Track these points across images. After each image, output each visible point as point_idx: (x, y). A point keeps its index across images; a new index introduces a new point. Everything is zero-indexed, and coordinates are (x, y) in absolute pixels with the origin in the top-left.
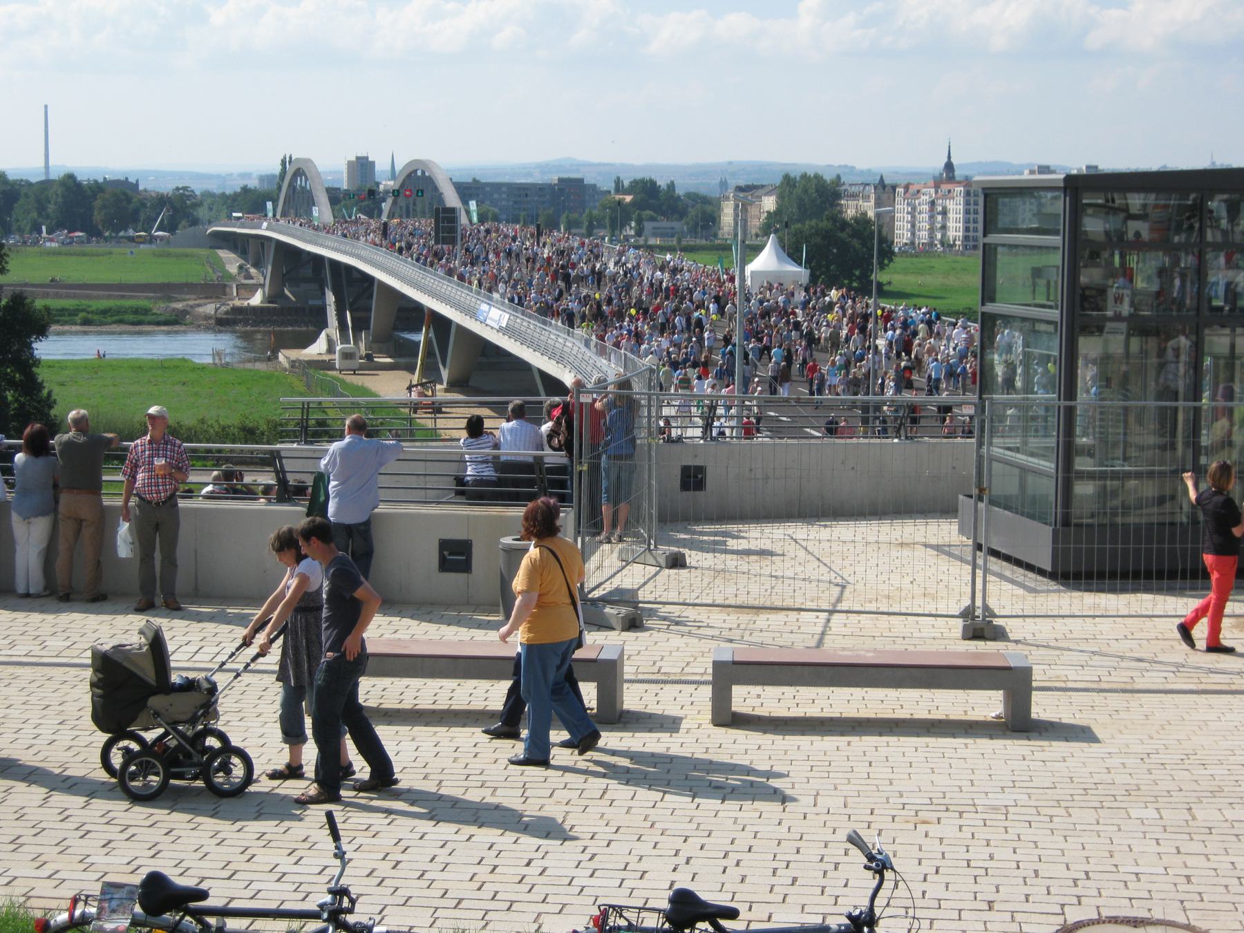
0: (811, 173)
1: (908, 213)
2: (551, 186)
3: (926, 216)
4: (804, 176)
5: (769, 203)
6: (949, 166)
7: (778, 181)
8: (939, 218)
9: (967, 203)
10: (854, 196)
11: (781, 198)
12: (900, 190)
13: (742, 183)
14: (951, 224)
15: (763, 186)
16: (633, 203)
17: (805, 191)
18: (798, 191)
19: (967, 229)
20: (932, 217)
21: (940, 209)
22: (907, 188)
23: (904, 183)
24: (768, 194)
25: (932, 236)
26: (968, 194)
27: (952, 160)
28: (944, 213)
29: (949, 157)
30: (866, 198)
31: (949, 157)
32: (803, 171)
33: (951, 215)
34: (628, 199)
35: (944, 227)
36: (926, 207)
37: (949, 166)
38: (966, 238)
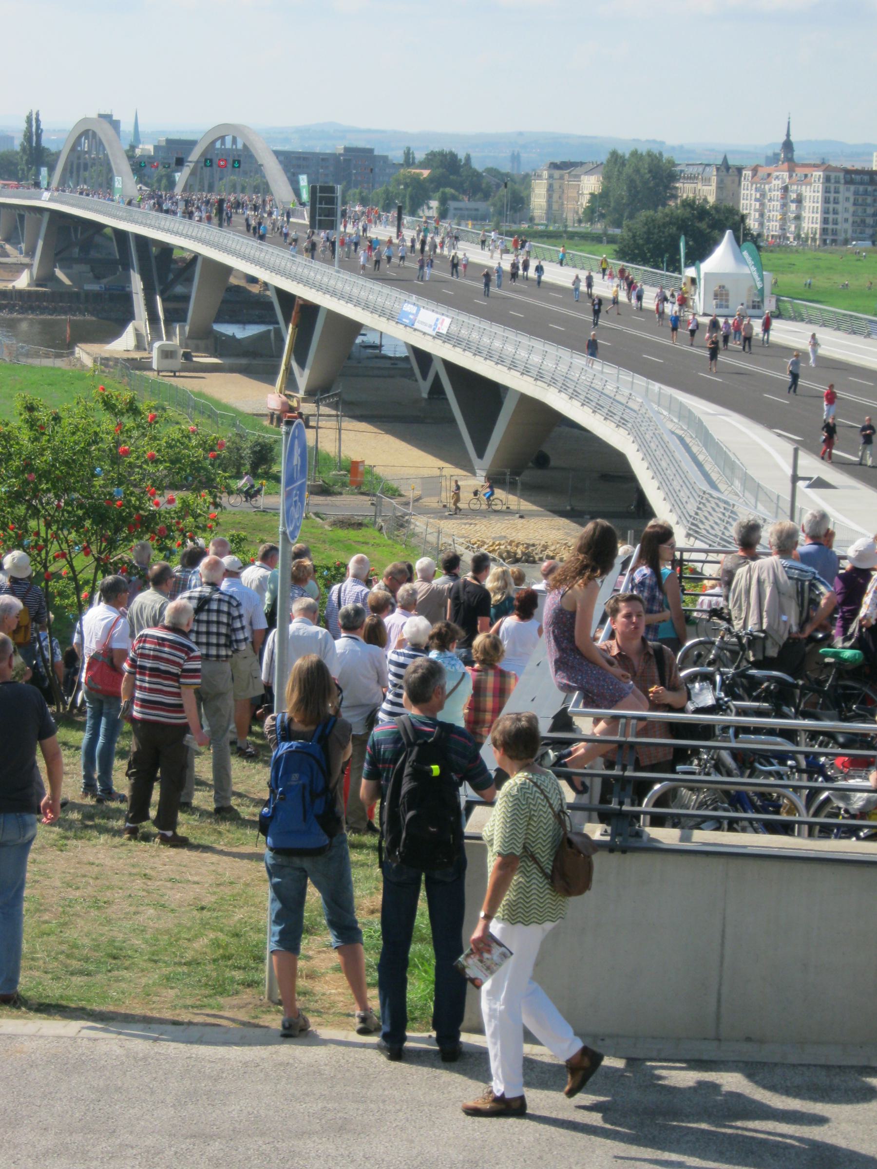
0: (643, 149)
1: (756, 200)
2: (335, 157)
3: (777, 204)
4: (634, 154)
5: (591, 184)
6: (788, 146)
7: (604, 158)
8: (793, 206)
9: (827, 191)
10: (692, 178)
11: (607, 177)
12: (747, 173)
13: (558, 161)
14: (806, 214)
15: (582, 164)
16: (431, 179)
17: (637, 171)
18: (628, 170)
19: (825, 221)
20: (784, 205)
21: (794, 196)
22: (755, 170)
23: (754, 163)
24: (589, 172)
25: (783, 228)
26: (827, 179)
27: (792, 138)
28: (799, 201)
29: (788, 135)
30: (707, 181)
31: (788, 135)
32: (611, 148)
33: (807, 204)
34: (426, 173)
35: (798, 218)
36: (778, 194)
37: (788, 146)
38: (824, 231)
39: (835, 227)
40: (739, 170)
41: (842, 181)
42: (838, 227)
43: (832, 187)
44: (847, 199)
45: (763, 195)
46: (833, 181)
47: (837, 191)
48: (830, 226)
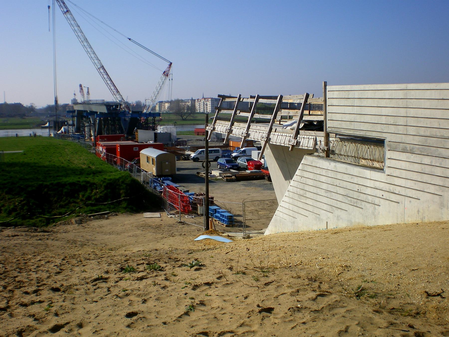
8: (206, 106)
9: (212, 103)
22: (198, 100)
28: (207, 105)
33: (208, 105)
35: (207, 108)
40: (195, 100)
43: (213, 102)
44: (216, 104)
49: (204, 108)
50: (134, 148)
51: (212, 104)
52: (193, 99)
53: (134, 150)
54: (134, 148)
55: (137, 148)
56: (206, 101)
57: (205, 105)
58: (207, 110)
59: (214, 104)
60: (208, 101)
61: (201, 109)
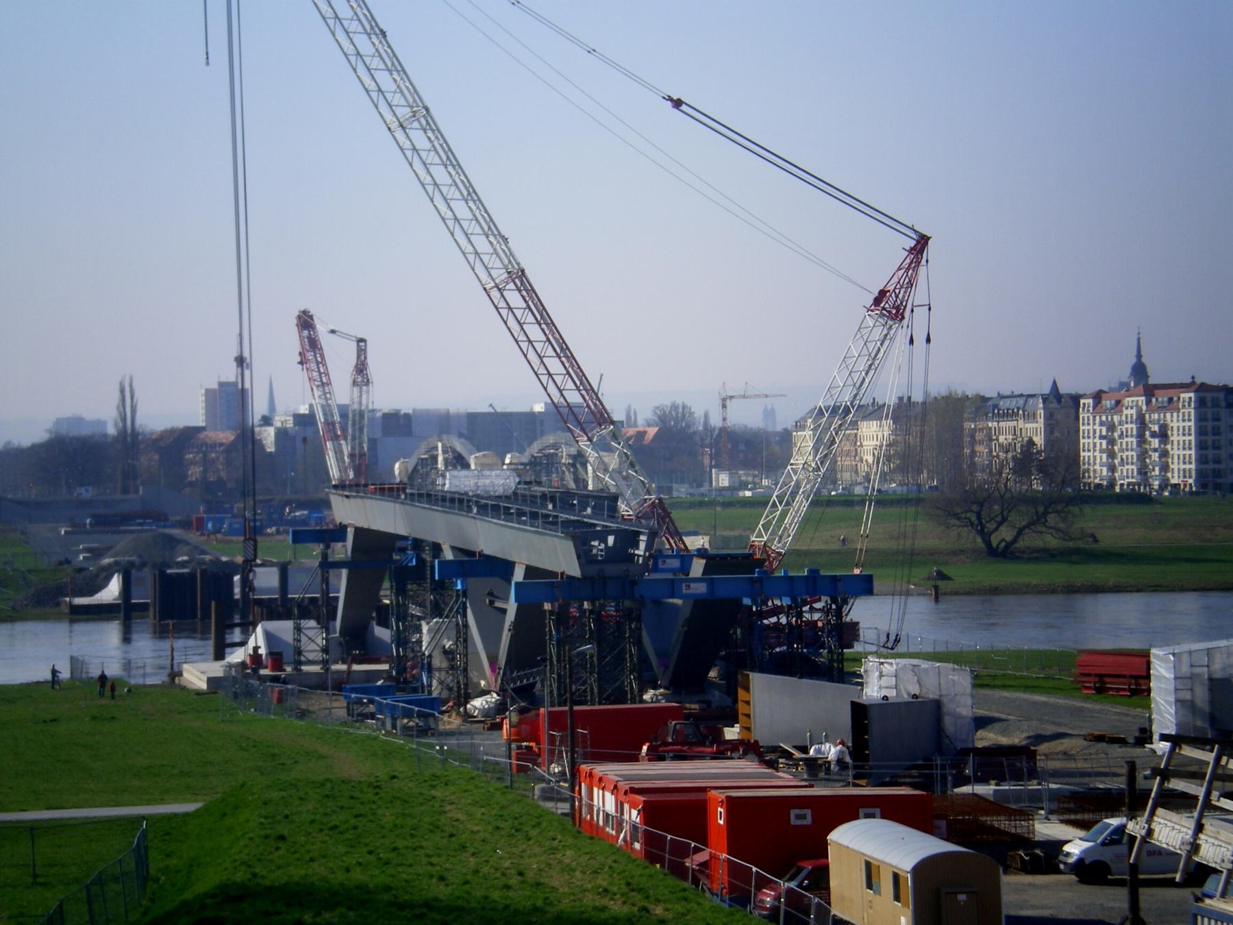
8: (1155, 443)
9: (1201, 419)
14: (1175, 451)
28: (1163, 435)
30: (1031, 417)
33: (1175, 437)
35: (1164, 454)
39: (1216, 466)
40: (1076, 399)
41: (1223, 404)
42: (1222, 466)
43: (1210, 413)
45: (1111, 427)
46: (1209, 404)
47: (1217, 419)
48: (1211, 466)
49: (1143, 456)
50: (794, 813)
51: (1201, 431)
52: (1061, 391)
53: (793, 821)
54: (794, 813)
55: (808, 812)
56: (1162, 409)
57: (1153, 435)
58: (1165, 468)
59: (1216, 431)
60: (1171, 404)
61: (1122, 463)
